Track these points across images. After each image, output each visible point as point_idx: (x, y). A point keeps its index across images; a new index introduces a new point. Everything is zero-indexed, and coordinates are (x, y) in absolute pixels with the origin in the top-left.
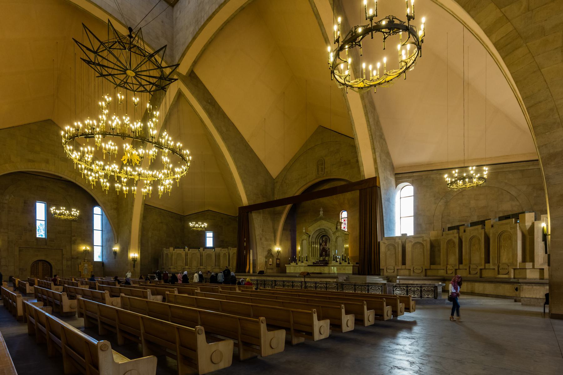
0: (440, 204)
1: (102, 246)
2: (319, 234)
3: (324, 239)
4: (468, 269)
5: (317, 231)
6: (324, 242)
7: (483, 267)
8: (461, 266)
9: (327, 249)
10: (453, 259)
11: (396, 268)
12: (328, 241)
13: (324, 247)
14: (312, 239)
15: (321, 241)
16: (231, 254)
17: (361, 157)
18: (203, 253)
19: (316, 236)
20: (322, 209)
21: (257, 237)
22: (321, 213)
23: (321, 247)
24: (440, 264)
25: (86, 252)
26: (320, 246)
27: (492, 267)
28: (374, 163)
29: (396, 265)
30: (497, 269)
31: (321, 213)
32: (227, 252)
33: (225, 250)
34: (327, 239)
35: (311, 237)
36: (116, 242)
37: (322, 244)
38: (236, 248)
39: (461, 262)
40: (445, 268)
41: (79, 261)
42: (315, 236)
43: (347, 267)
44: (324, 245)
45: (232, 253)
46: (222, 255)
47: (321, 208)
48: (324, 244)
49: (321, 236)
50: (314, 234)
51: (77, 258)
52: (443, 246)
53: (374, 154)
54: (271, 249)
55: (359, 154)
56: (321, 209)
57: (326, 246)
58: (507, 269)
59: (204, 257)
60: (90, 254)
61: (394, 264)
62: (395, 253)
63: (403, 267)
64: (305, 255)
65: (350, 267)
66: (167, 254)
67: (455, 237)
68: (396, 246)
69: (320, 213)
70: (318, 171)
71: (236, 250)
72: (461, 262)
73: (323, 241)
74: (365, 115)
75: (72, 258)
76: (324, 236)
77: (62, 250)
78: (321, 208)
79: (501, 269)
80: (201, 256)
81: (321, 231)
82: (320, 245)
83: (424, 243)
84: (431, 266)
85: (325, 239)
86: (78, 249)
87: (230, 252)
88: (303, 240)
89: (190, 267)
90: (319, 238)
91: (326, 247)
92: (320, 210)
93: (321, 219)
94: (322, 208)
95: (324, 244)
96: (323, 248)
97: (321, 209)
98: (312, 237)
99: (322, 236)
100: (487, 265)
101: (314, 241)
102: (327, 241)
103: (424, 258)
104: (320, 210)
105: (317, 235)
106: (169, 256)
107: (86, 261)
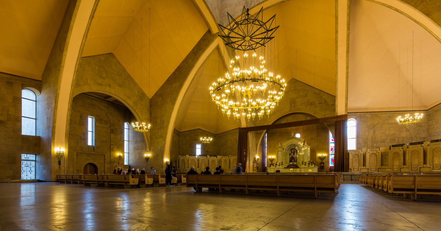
0: (371, 132)
1: (129, 153)
2: (290, 147)
3: (292, 151)
4: (410, 168)
6: (292, 153)
7: (422, 166)
8: (405, 166)
9: (295, 158)
10: (397, 163)
11: (359, 168)
12: (296, 152)
13: (293, 156)
14: (285, 151)
15: (290, 152)
16: (231, 160)
17: (337, 102)
18: (210, 159)
19: (288, 149)
21: (250, 149)
23: (291, 156)
24: (388, 165)
25: (120, 157)
26: (289, 156)
27: (428, 166)
28: (345, 106)
29: (359, 166)
30: (432, 167)
32: (227, 159)
33: (226, 157)
34: (295, 151)
35: (284, 150)
36: (148, 150)
38: (236, 156)
39: (404, 164)
40: (392, 168)
41: (115, 164)
42: (287, 149)
43: (314, 169)
44: (293, 155)
45: (232, 159)
46: (223, 160)
48: (293, 154)
49: (291, 149)
50: (287, 147)
51: (114, 162)
52: (390, 155)
53: (346, 101)
54: (255, 157)
55: (337, 100)
57: (294, 155)
58: (439, 167)
59: (210, 162)
60: (121, 159)
61: (358, 166)
62: (359, 160)
63: (364, 167)
64: (280, 161)
65: (316, 168)
66: (183, 160)
67: (400, 151)
68: (360, 155)
70: (291, 107)
71: (237, 157)
72: (404, 164)
73: (292, 152)
74: (346, 78)
75: (111, 162)
76: (292, 149)
77: (105, 155)
79: (435, 167)
80: (209, 161)
81: (291, 146)
82: (290, 154)
83: (377, 154)
84: (382, 166)
86: (114, 155)
87: (231, 159)
88: (278, 152)
89: (200, 169)
90: (289, 150)
91: (294, 156)
95: (292, 154)
96: (292, 157)
98: (285, 150)
99: (291, 149)
100: (424, 165)
101: (286, 152)
102: (295, 152)
103: (377, 162)
105: (289, 148)
106: (186, 161)
107: (120, 164)
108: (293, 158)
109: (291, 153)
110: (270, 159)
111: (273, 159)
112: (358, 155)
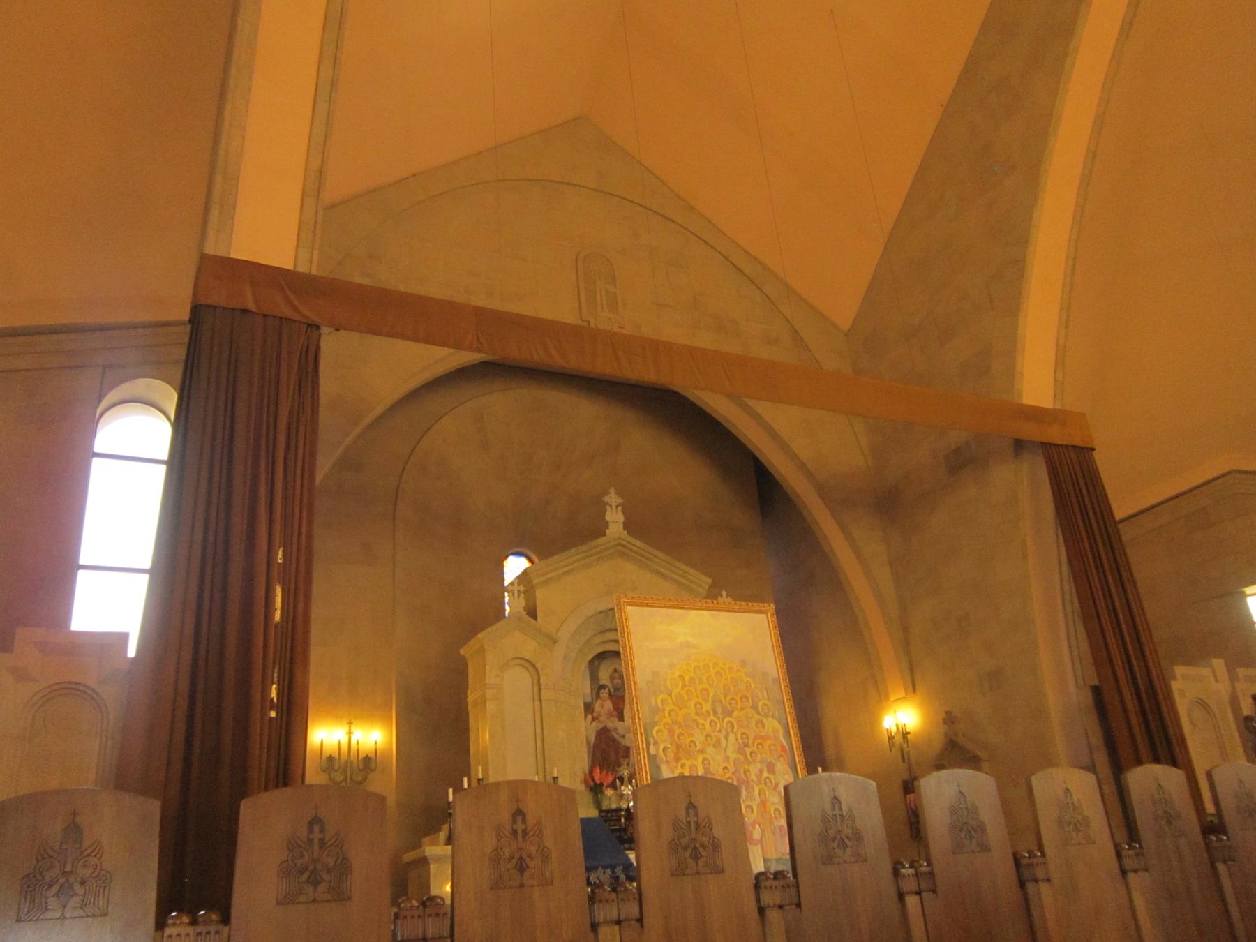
5: (591, 617)
6: (604, 693)
13: (610, 725)
15: (587, 688)
20: (620, 500)
22: (615, 518)
31: (615, 518)
37: (597, 707)
47: (612, 491)
48: (609, 705)
56: (613, 498)
57: (621, 718)
69: (609, 516)
73: (598, 688)
78: (612, 491)
82: (588, 708)
85: (612, 678)
91: (618, 724)
92: (606, 499)
93: (621, 551)
94: (619, 494)
95: (604, 706)
96: (603, 734)
97: (613, 498)
99: (591, 662)
104: (606, 499)
108: (614, 740)
109: (598, 696)
110: (330, 759)
111: (367, 759)
112: (1203, 705)
